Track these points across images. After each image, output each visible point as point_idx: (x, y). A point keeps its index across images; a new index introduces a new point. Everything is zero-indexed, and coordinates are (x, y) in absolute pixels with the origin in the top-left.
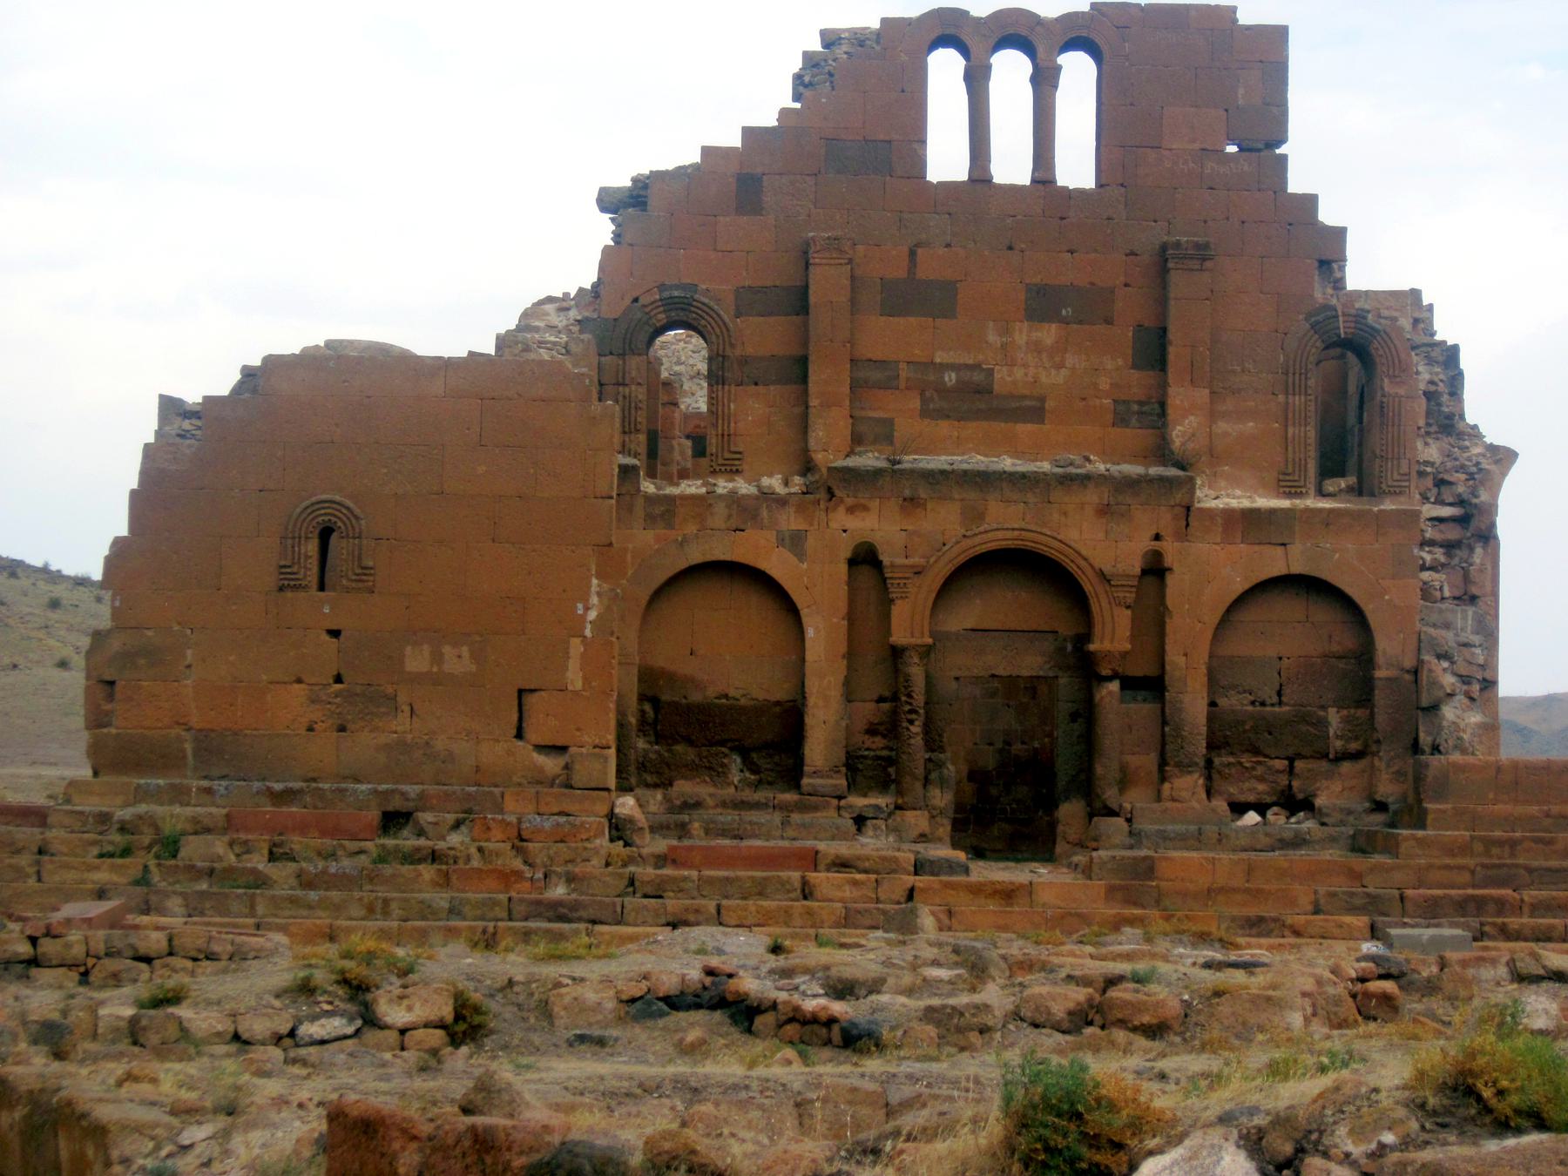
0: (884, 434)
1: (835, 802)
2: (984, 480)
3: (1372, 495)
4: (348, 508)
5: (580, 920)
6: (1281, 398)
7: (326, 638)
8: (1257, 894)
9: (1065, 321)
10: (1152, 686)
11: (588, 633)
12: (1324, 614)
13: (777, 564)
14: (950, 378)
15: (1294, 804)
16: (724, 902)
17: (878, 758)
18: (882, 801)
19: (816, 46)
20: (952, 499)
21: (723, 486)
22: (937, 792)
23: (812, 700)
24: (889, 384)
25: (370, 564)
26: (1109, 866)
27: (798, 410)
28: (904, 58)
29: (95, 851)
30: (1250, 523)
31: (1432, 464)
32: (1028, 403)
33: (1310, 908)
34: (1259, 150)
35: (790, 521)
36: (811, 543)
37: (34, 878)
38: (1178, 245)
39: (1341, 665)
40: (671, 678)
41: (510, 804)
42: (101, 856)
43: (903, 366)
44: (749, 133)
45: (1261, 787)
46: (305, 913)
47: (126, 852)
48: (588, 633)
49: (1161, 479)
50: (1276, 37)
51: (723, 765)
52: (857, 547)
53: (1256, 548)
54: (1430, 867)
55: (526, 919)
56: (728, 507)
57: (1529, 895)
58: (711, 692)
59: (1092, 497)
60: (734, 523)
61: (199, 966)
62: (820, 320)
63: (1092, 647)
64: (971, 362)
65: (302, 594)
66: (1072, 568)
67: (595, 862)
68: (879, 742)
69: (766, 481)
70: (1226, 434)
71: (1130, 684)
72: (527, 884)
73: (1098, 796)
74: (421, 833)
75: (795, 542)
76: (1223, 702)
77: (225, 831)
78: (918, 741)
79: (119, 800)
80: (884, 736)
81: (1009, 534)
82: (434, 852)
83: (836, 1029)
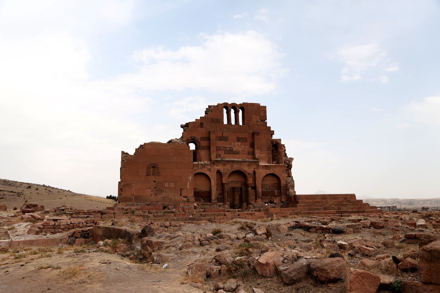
0: (219, 156)
1: (216, 204)
2: (233, 162)
3: (279, 163)
4: (156, 164)
5: (195, 220)
6: (268, 151)
7: (153, 182)
8: (283, 213)
9: (242, 142)
10: (254, 188)
11: (190, 181)
12: (274, 179)
13: (207, 173)
14: (228, 149)
15: (271, 202)
16: (215, 217)
17: (221, 198)
18: (222, 204)
19: (208, 107)
20: (229, 164)
21: (200, 163)
22: (228, 202)
23: (212, 191)
24: (220, 150)
25: (160, 172)
26: (263, 210)
27: (209, 153)
28: (221, 109)
29: (122, 213)
30: (266, 166)
32: (237, 152)
33: (289, 214)
34: (263, 121)
36: (212, 169)
37: (114, 217)
38: (255, 132)
39: (276, 185)
41: (181, 204)
42: (123, 214)
43: (222, 147)
44: (201, 117)
45: (267, 200)
46: (156, 221)
47: (127, 213)
48: (190, 181)
49: (255, 161)
50: (265, 107)
51: (200, 200)
52: (218, 170)
53: (266, 170)
55: (188, 220)
56: (201, 165)
57: (316, 212)
58: (198, 190)
59: (247, 164)
60: (202, 167)
61: (174, 228)
62: (212, 141)
63: (248, 183)
64: (230, 147)
65: (150, 176)
66: (245, 173)
67: (195, 212)
68: (220, 196)
69: (205, 162)
71: (252, 188)
72: (187, 216)
73: (249, 202)
74: (169, 209)
75: (210, 170)
76: (263, 190)
77: (141, 210)
78: (226, 195)
79: (124, 206)
80: (221, 195)
81: (237, 168)
82: (172, 212)
83: (331, 230)
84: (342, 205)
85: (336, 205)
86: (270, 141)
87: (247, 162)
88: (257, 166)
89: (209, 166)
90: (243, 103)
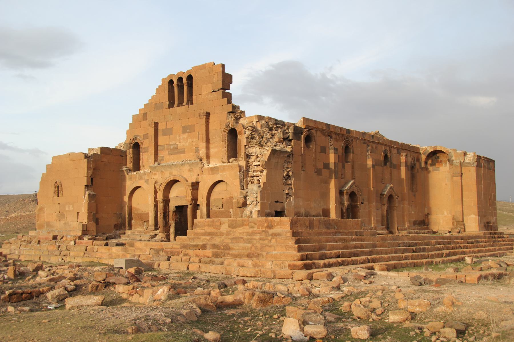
2: (170, 166)
14: (172, 147)
23: (150, 212)
30: (214, 170)
31: (256, 153)
32: (183, 150)
35: (146, 178)
40: (136, 209)
43: (165, 145)
44: (145, 105)
53: (213, 175)
54: (173, 244)
59: (187, 167)
60: (140, 179)
64: (174, 143)
70: (213, 152)
75: (147, 181)
81: (174, 177)
84: (242, 240)
85: (232, 241)
86: (226, 124)
87: (187, 165)
88: (200, 170)
89: (146, 175)
90: (192, 68)
